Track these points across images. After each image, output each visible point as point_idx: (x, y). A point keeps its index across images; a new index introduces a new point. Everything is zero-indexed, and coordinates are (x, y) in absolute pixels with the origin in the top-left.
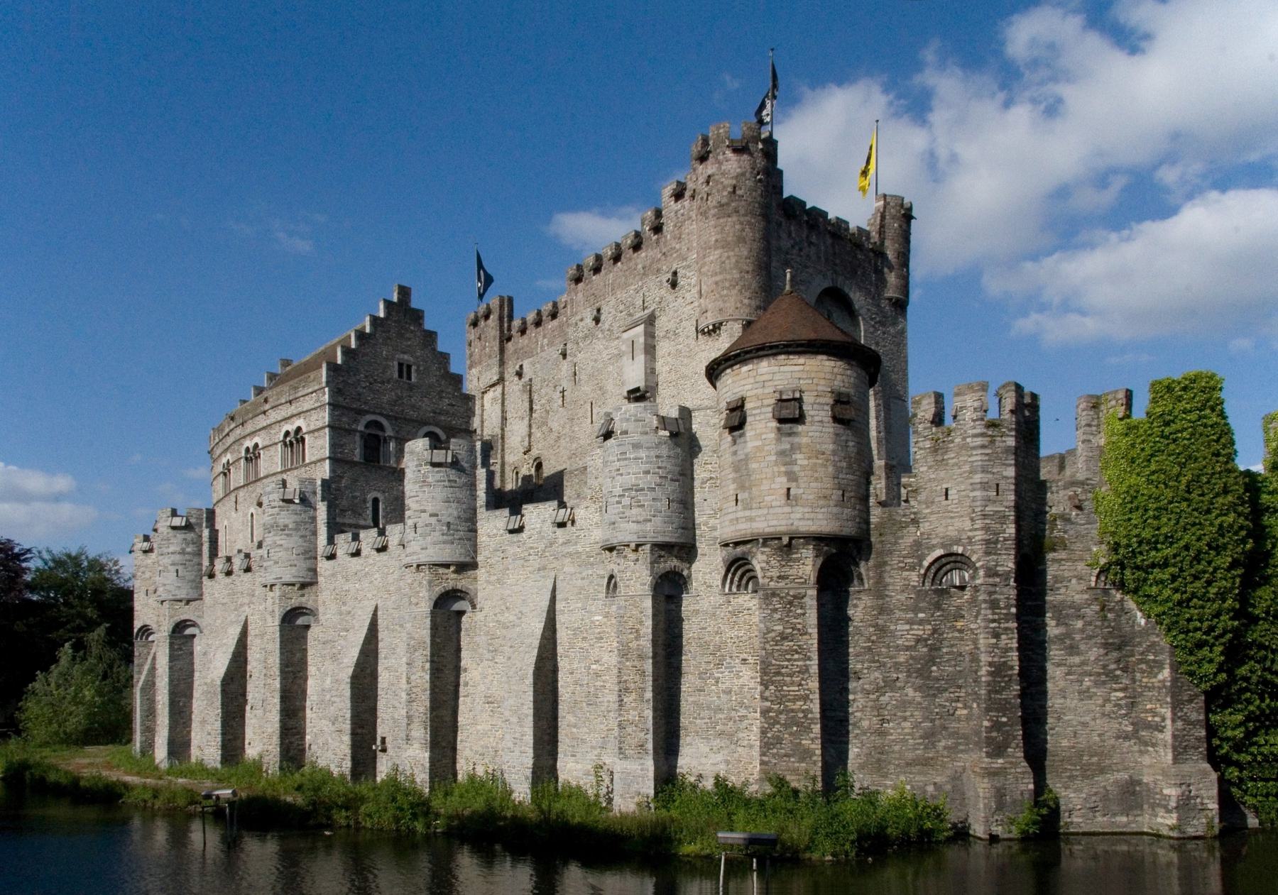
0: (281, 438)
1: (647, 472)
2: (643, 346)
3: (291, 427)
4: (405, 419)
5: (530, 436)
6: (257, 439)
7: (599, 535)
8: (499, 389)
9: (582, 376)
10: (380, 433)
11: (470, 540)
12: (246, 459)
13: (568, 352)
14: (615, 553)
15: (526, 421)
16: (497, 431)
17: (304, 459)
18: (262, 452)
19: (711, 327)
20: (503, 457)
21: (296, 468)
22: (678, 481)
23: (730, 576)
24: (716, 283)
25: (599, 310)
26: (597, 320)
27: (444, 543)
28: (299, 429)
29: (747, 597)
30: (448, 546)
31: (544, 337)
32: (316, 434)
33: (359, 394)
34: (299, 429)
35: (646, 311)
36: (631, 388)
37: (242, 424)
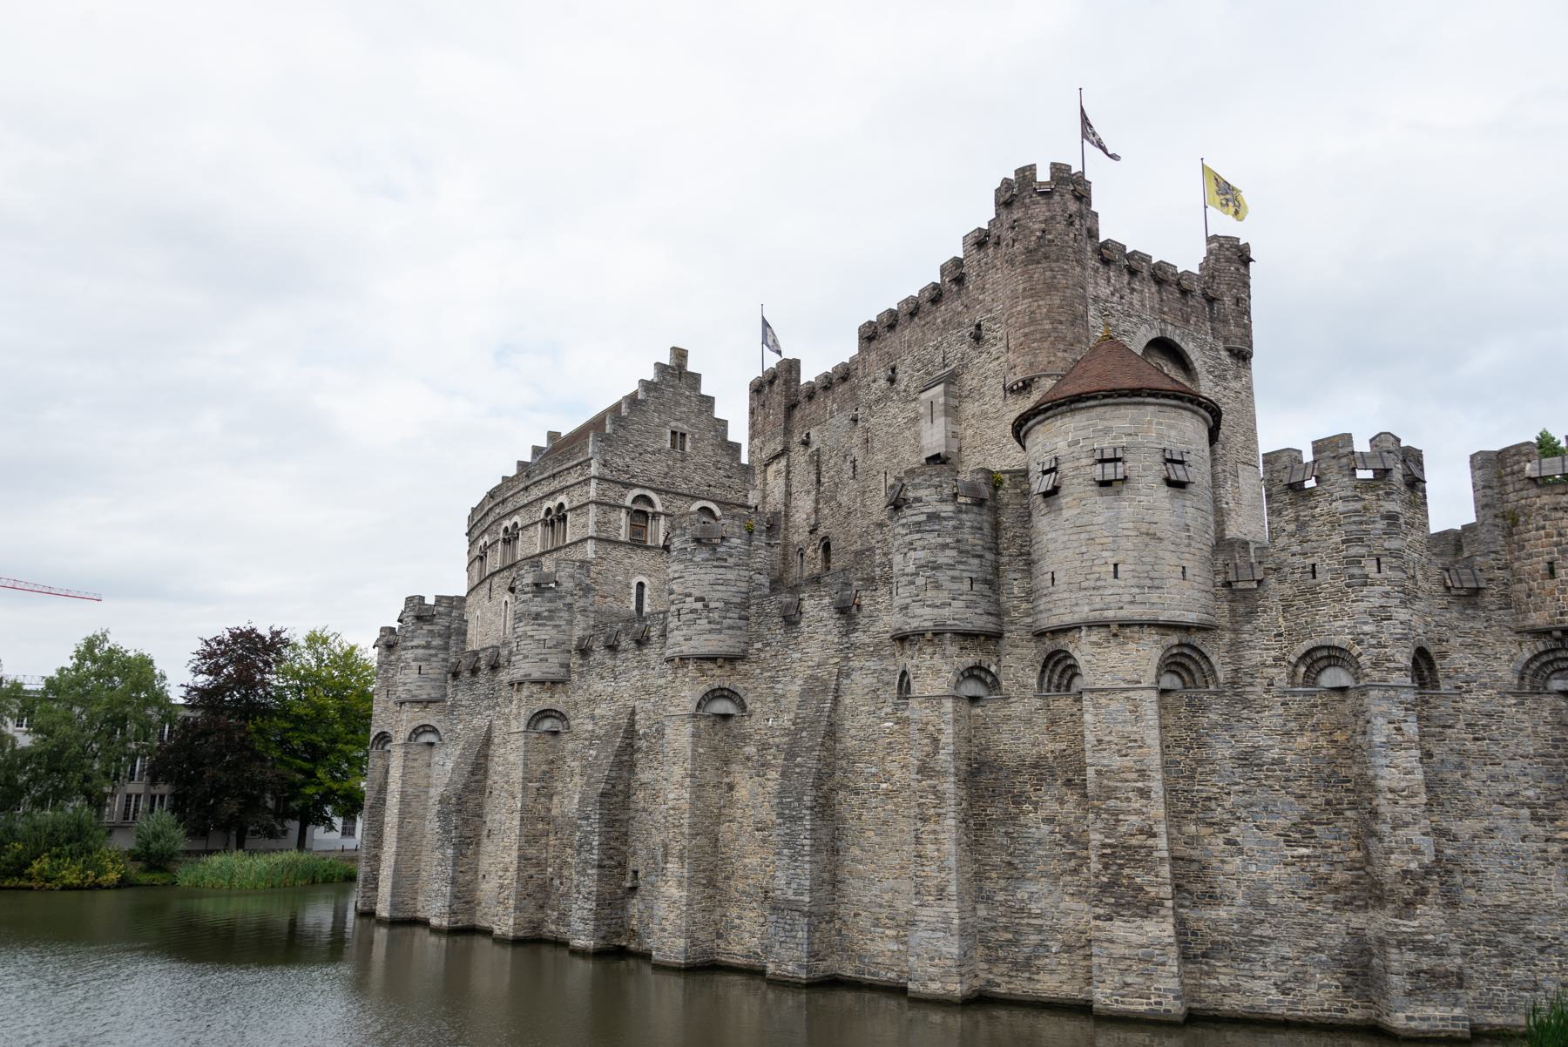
0: (542, 517)
1: (945, 546)
2: (942, 408)
3: (551, 504)
4: (677, 494)
5: (817, 511)
6: (516, 518)
7: (891, 621)
8: (783, 462)
9: (877, 445)
10: (649, 510)
11: (740, 628)
12: (504, 540)
13: (860, 416)
14: (907, 645)
15: (813, 496)
16: (781, 507)
17: (565, 540)
18: (520, 532)
19: (1020, 384)
20: (786, 538)
21: (556, 550)
22: (980, 557)
23: (1048, 672)
24: (1026, 335)
25: (893, 370)
26: (892, 380)
27: (710, 631)
28: (561, 505)
29: (1070, 700)
30: (715, 636)
31: (834, 401)
32: (579, 511)
33: (628, 466)
34: (561, 505)
35: (947, 369)
36: (930, 454)
37: (503, 502)
